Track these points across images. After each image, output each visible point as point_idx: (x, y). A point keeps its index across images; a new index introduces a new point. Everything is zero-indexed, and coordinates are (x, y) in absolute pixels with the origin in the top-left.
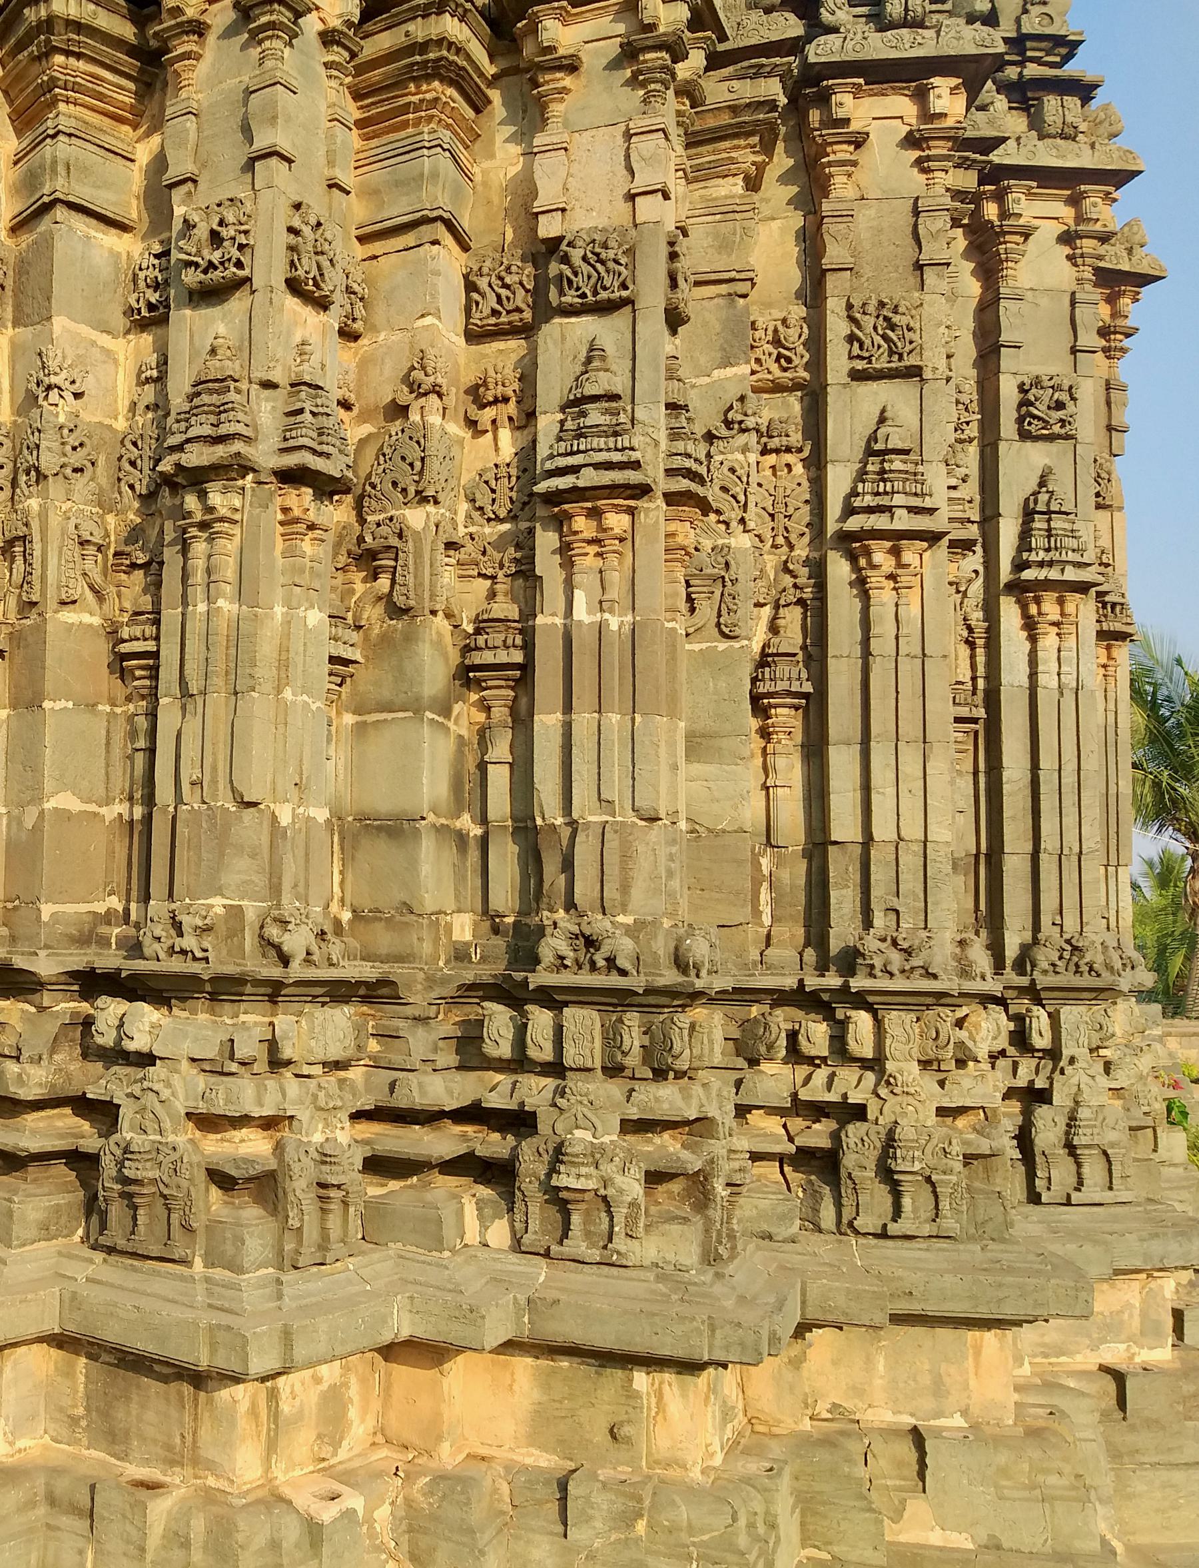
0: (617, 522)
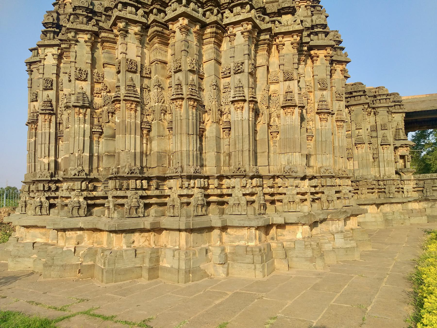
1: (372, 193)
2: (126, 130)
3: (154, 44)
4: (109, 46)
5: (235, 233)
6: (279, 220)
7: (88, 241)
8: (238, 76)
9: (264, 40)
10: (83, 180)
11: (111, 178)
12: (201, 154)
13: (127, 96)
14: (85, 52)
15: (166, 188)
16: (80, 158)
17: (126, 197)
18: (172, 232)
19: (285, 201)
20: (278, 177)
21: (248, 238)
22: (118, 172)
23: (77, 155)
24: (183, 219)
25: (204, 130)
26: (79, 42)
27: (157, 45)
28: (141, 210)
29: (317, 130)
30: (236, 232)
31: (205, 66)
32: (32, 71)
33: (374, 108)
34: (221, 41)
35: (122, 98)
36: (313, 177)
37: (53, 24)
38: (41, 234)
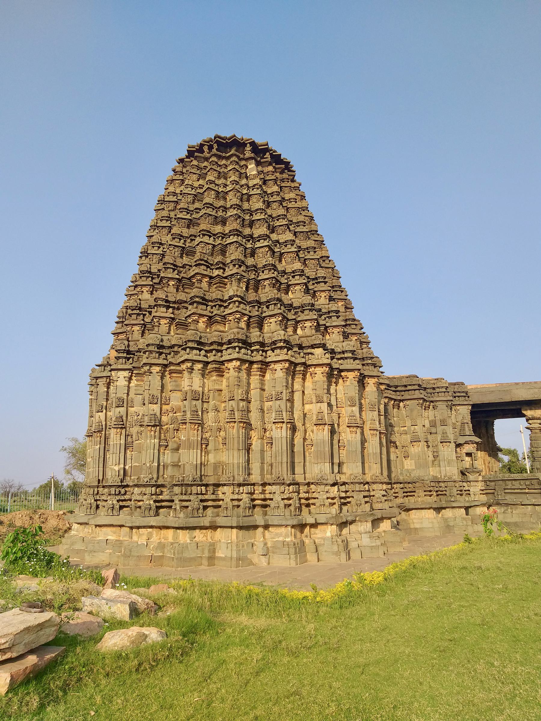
0: (184, 426)
1: (431, 496)
2: (190, 446)
6: (311, 520)
7: (156, 536)
8: (278, 402)
9: (300, 371)
10: (153, 486)
11: (176, 485)
12: (248, 464)
15: (220, 493)
16: (150, 467)
17: (190, 501)
18: (225, 529)
19: (317, 504)
20: (312, 483)
21: (283, 535)
22: (183, 480)
23: (148, 465)
24: (235, 519)
25: (251, 445)
27: (214, 378)
28: (201, 511)
29: (348, 441)
31: (252, 392)
33: (432, 402)
34: (265, 373)
35: (188, 421)
36: (344, 484)
37: (125, 350)
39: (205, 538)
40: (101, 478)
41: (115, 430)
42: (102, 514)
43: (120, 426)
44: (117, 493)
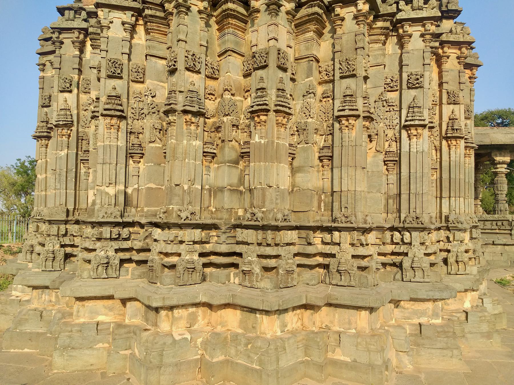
0: (263, 118)
3: (304, 32)
4: (235, 25)
5: (413, 307)
13: (280, 105)
14: (198, 28)
17: (277, 257)
23: (186, 187)
26: (191, 11)
27: (311, 34)
30: (413, 305)
32: (62, 43)
35: (272, 107)
38: (105, 308)
39: (299, 324)
40: (71, 207)
41: (108, 120)
42: (85, 274)
43: (119, 113)
44: (114, 236)
